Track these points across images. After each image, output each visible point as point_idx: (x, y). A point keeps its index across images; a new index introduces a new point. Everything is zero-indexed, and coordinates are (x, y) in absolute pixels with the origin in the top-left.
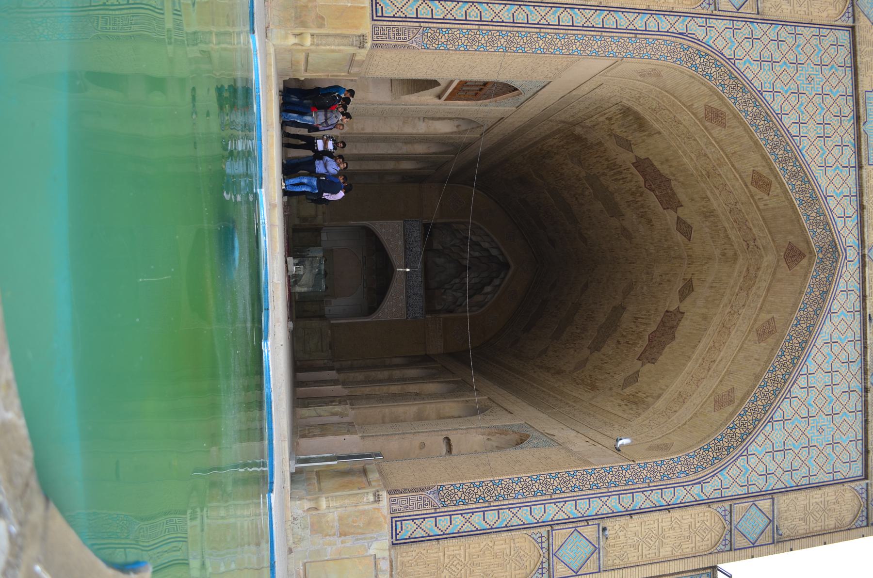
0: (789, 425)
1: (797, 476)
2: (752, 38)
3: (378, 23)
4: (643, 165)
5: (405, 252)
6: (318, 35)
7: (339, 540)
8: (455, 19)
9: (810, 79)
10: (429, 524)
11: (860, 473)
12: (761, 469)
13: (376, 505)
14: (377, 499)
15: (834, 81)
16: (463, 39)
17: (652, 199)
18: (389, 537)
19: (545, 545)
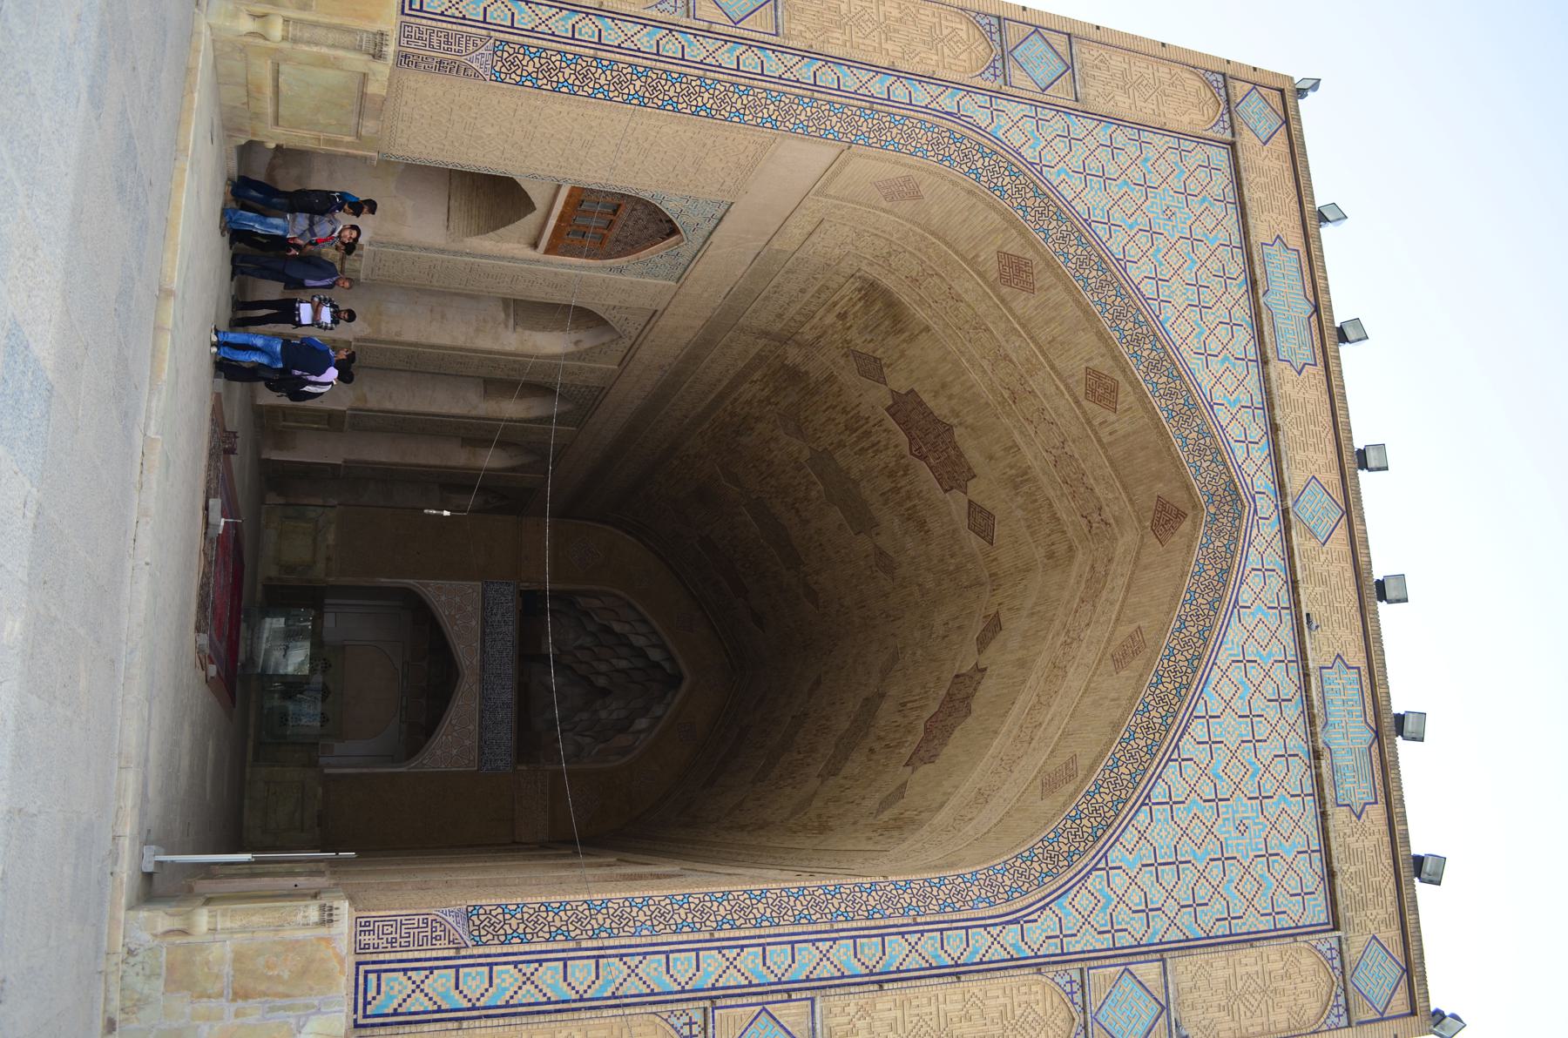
0: (1181, 813)
1: (1206, 917)
2: (1067, 136)
3: (413, 20)
4: (906, 408)
5: (483, 641)
6: (297, 22)
8: (553, 34)
9: (1169, 213)
10: (441, 982)
11: (1323, 918)
13: (323, 931)
14: (328, 918)
15: (1210, 222)
16: (567, 71)
17: (924, 476)
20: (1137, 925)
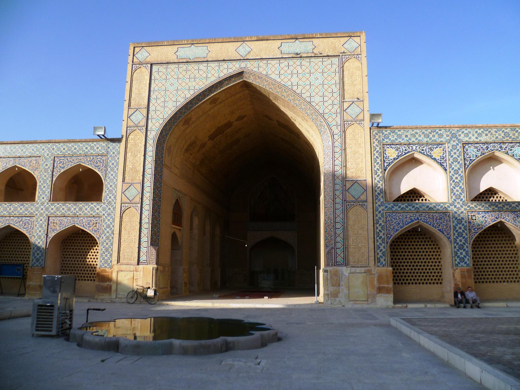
0: (313, 94)
1: (335, 90)
2: (155, 111)
4: (212, 137)
7: (341, 287)
9: (172, 84)
12: (330, 107)
13: (329, 272)
15: (173, 73)
18: (342, 267)
19: (352, 203)
20: (336, 107)
